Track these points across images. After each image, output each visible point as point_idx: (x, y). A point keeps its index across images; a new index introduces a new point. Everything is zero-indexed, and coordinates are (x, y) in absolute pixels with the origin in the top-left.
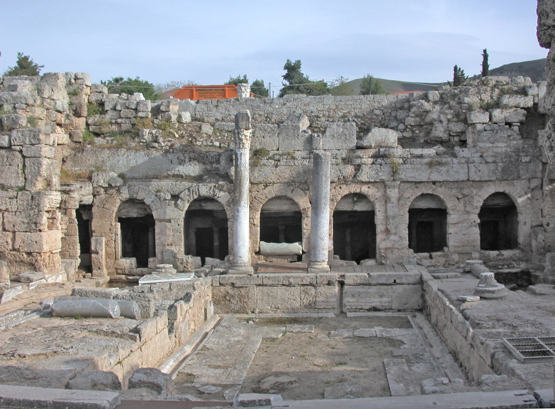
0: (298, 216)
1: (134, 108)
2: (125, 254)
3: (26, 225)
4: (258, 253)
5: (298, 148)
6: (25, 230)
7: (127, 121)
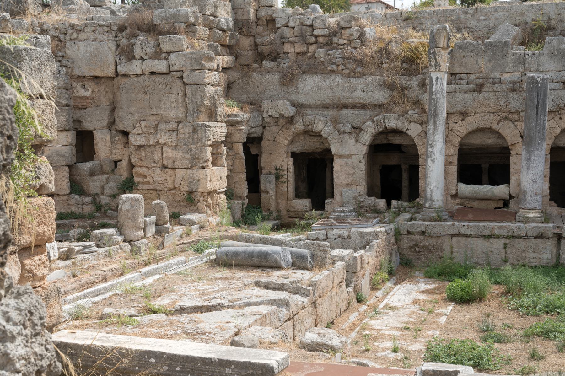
0: (505, 152)
4: (455, 196)
5: (507, 70)
6: (186, 167)
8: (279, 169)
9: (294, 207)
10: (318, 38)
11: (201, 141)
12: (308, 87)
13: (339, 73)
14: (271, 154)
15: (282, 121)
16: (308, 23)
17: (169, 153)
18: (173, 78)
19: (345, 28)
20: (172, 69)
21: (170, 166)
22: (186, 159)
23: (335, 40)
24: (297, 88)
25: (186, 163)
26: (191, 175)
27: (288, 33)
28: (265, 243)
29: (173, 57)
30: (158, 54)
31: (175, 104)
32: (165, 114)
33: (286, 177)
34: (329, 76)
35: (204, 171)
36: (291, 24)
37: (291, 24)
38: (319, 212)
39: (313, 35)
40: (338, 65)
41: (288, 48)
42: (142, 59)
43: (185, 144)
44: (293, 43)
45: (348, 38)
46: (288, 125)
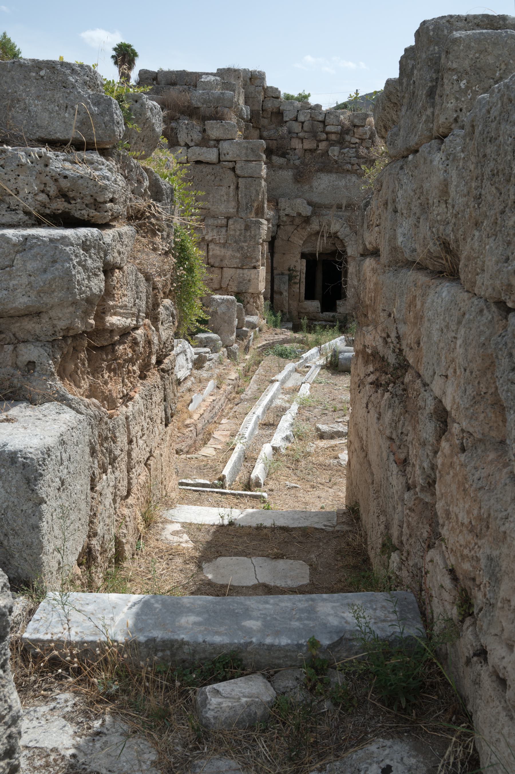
6: (235, 266)
8: (292, 270)
9: (305, 309)
10: (330, 135)
11: (255, 239)
12: (323, 186)
13: (354, 173)
14: (284, 254)
15: (297, 221)
16: (321, 118)
17: (216, 250)
18: (224, 169)
19: (358, 127)
20: (223, 158)
21: (217, 264)
22: (236, 258)
23: (348, 138)
24: (311, 187)
25: (236, 262)
26: (241, 275)
27: (296, 127)
29: (225, 146)
30: (205, 142)
31: (225, 197)
32: (213, 208)
33: (298, 278)
34: (344, 175)
35: (255, 271)
36: (301, 118)
37: (301, 118)
38: (332, 314)
39: (324, 131)
40: (353, 165)
41: (296, 144)
42: (188, 146)
43: (235, 242)
44: (302, 139)
45: (360, 137)
46: (304, 225)
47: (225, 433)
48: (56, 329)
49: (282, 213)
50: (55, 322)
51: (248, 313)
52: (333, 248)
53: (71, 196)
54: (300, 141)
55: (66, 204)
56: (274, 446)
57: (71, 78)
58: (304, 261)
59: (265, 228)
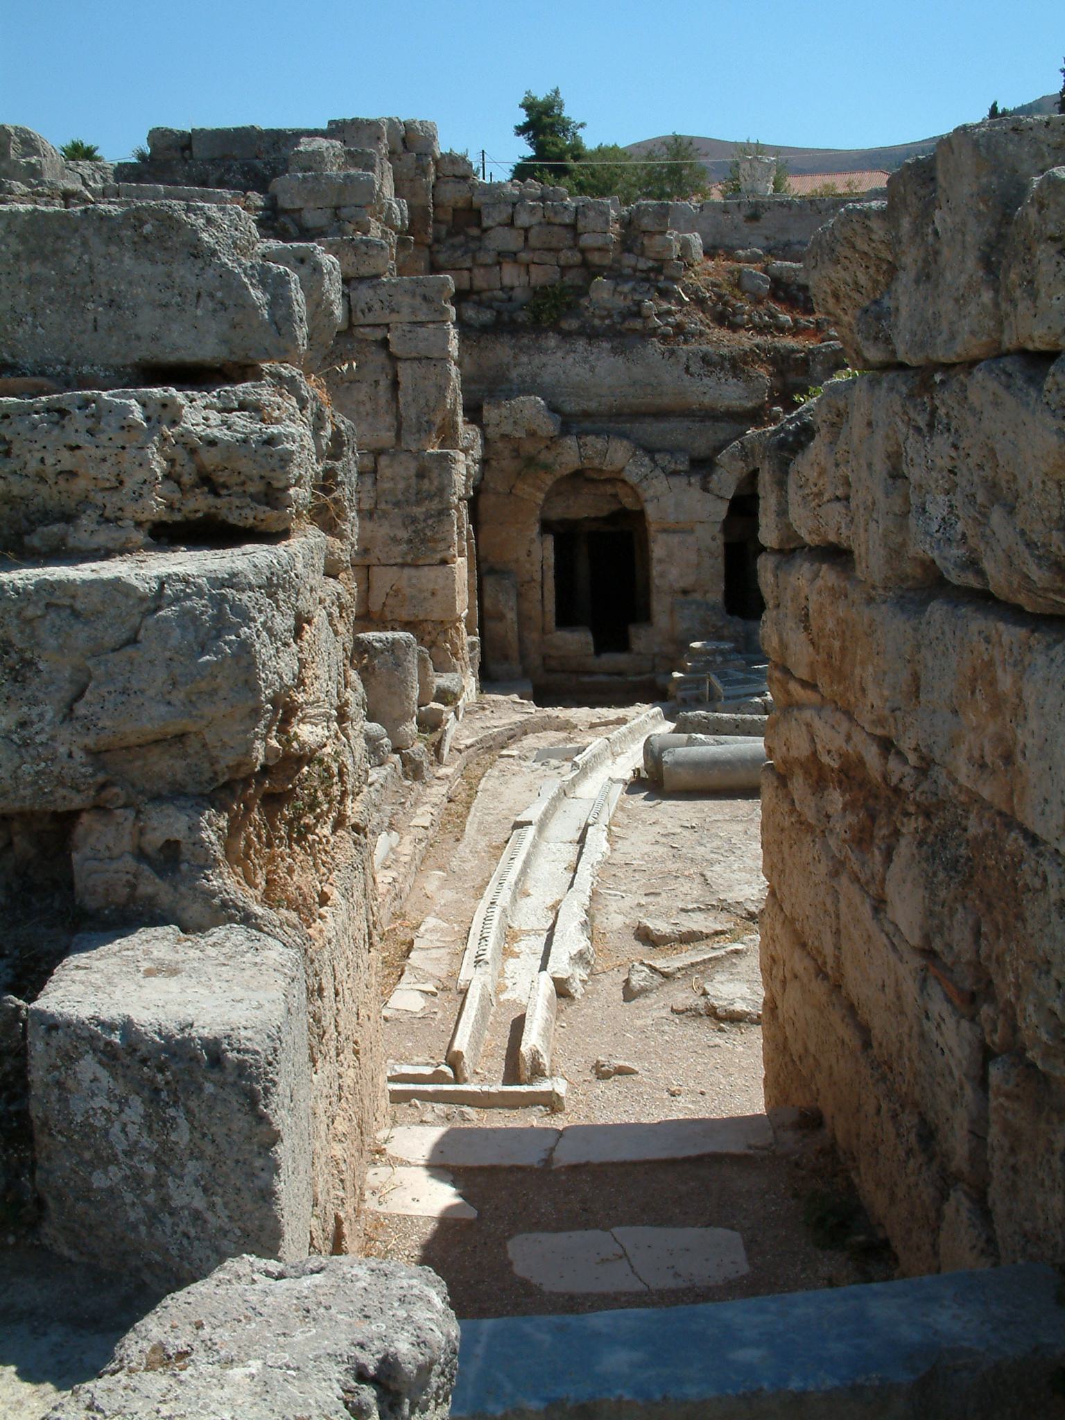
1: (567, 221)
2: (565, 618)
3: (404, 547)
6: (399, 560)
7: (548, 257)
19: (650, 234)
20: (359, 318)
28: (749, 734)
36: (523, 219)
37: (523, 219)
47: (434, 953)
48: (218, 767)
49: (492, 432)
50: (215, 753)
51: (441, 668)
52: (614, 507)
53: (222, 480)
54: (523, 270)
55: (211, 500)
56: (557, 976)
57: (205, 236)
58: (550, 542)
59: (463, 468)
